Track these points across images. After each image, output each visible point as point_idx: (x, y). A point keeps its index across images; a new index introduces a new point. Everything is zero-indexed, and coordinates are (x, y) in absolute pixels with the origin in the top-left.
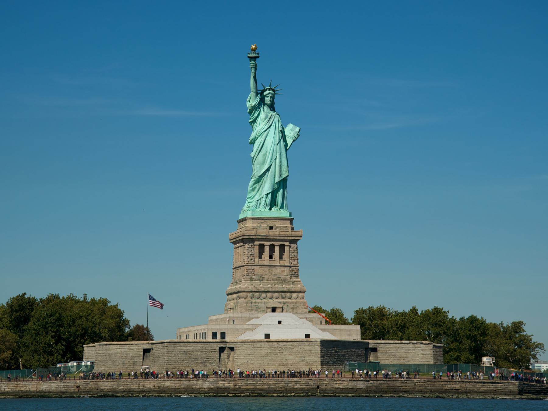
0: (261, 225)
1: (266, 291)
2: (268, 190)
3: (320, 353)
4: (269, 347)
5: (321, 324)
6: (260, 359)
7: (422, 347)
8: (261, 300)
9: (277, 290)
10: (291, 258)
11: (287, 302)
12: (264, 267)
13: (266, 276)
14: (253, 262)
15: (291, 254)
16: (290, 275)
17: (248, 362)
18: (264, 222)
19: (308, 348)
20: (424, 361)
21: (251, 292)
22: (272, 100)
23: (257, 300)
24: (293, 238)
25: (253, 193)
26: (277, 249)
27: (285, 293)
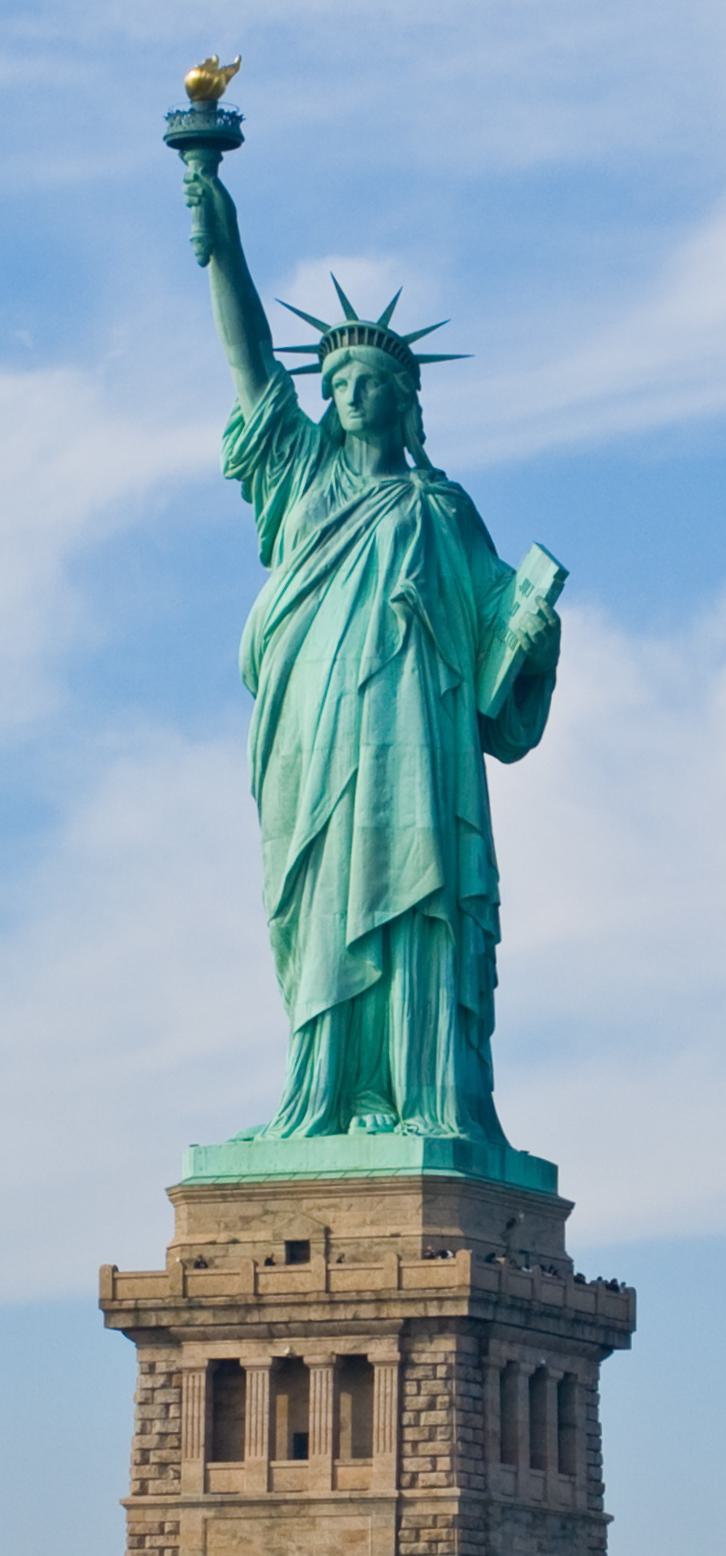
2: (309, 1001)
15: (408, 1417)
22: (367, 404)
26: (320, 1386)
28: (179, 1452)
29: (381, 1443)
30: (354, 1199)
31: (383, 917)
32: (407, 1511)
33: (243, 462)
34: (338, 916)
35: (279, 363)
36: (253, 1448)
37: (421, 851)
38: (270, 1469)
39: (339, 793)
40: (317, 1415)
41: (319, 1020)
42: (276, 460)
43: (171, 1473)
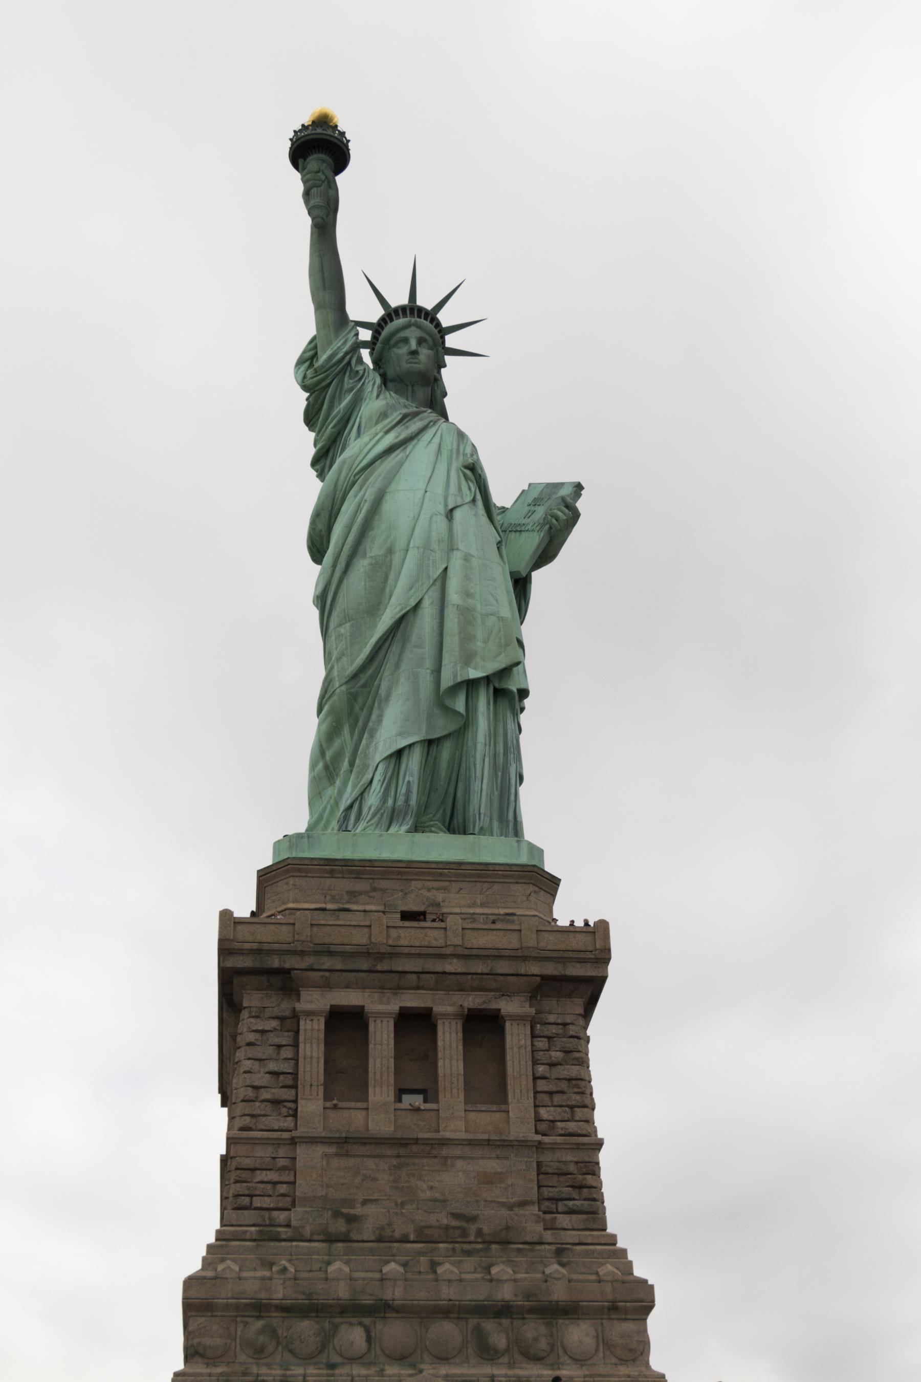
1: (367, 1301)
2: (401, 734)
8: (332, 1366)
9: (448, 1293)
10: (545, 1098)
12: (363, 1150)
13: (370, 1210)
14: (289, 1122)
15: (541, 1069)
16: (547, 1203)
18: (366, 893)
21: (259, 1308)
23: (299, 1371)
24: (551, 969)
25: (331, 791)
27: (505, 1322)
28: (293, 1092)
29: (518, 1091)
30: (464, 883)
31: (474, 674)
32: (547, 1157)
33: (325, 372)
34: (429, 671)
36: (378, 1089)
37: (502, 633)
38: (395, 1109)
39: (431, 582)
40: (447, 1061)
41: (406, 752)
42: (352, 374)
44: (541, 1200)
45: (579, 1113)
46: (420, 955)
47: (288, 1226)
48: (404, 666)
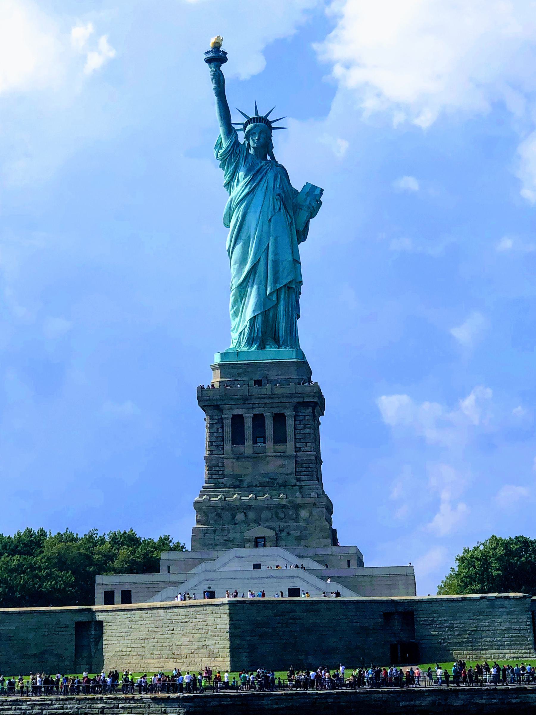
0: (237, 379)
2: (254, 311)
3: (228, 630)
4: (152, 619)
5: (349, 566)
6: (139, 645)
7: (508, 606)
8: (236, 524)
11: (287, 527)
13: (245, 478)
17: (123, 651)
18: (244, 373)
19: (210, 619)
20: (512, 637)
22: (261, 140)
25: (237, 320)
31: (278, 286)
35: (234, 128)
38: (253, 447)
41: (257, 316)
43: (220, 448)
44: (296, 472)
45: (309, 444)
46: (259, 398)
47: (223, 483)
48: (255, 284)
